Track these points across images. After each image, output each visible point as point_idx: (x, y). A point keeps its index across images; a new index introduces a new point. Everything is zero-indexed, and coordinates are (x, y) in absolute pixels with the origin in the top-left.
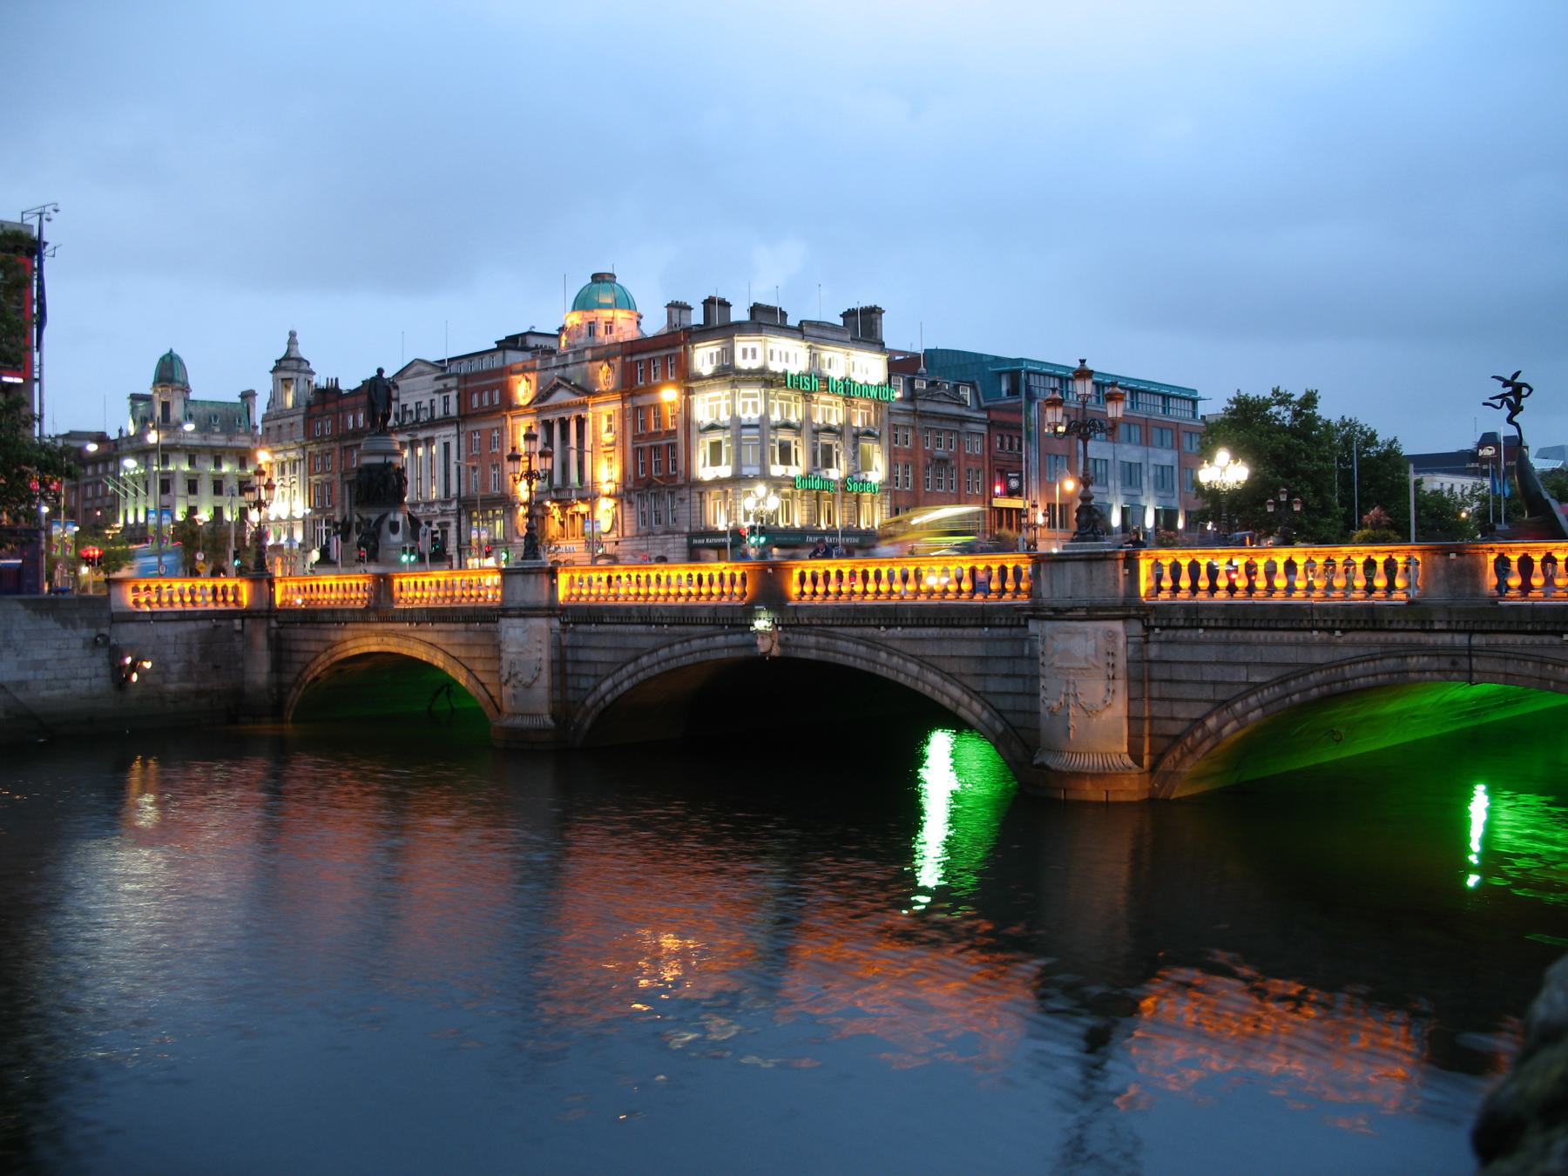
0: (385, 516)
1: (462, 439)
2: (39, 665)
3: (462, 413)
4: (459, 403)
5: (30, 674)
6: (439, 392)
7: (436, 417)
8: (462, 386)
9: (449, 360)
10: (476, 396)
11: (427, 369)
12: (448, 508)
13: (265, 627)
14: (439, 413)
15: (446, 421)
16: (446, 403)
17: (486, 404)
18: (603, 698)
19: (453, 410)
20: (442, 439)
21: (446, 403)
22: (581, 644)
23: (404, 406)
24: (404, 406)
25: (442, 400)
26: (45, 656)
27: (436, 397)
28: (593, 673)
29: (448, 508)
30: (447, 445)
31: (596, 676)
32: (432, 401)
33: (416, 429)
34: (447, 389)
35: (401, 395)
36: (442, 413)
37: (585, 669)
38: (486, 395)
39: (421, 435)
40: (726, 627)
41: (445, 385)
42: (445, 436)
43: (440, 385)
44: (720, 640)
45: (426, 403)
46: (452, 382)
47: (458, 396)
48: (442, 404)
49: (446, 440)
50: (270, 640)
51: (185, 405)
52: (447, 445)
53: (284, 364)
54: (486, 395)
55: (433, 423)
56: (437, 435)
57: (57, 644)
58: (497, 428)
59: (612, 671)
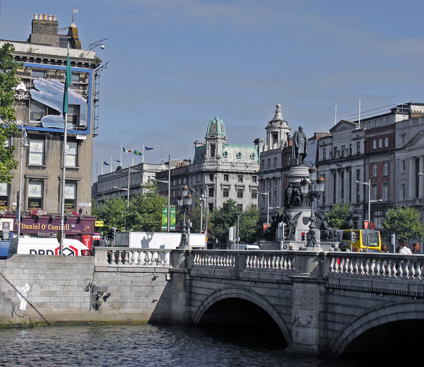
0: (300, 214)
1: (367, 168)
2: (52, 294)
3: (367, 152)
4: (365, 146)
5: (46, 299)
6: (355, 139)
7: (353, 155)
8: (367, 136)
9: (363, 121)
10: (375, 142)
11: (348, 126)
12: (358, 209)
13: (183, 279)
14: (354, 152)
15: (358, 157)
16: (358, 147)
17: (381, 146)
18: (347, 338)
19: (362, 151)
20: (355, 167)
21: (358, 147)
22: (336, 302)
23: (336, 148)
24: (336, 148)
25: (356, 144)
26: (56, 289)
27: (353, 142)
28: (342, 321)
29: (358, 209)
30: (358, 171)
31: (343, 323)
32: (351, 145)
33: (341, 161)
34: (358, 138)
35: (334, 142)
36: (356, 152)
37: (337, 318)
38: (381, 141)
39: (345, 165)
40: (415, 298)
41: (358, 136)
42: (357, 166)
43: (354, 136)
44: (412, 307)
45: (347, 147)
46: (362, 134)
47: (365, 142)
48: (356, 147)
49: (358, 168)
50: (185, 286)
51: (223, 147)
52: (358, 171)
53: (273, 124)
54: (381, 141)
55: (350, 158)
56: (353, 165)
57: (62, 283)
58: (387, 161)
59: (352, 321)
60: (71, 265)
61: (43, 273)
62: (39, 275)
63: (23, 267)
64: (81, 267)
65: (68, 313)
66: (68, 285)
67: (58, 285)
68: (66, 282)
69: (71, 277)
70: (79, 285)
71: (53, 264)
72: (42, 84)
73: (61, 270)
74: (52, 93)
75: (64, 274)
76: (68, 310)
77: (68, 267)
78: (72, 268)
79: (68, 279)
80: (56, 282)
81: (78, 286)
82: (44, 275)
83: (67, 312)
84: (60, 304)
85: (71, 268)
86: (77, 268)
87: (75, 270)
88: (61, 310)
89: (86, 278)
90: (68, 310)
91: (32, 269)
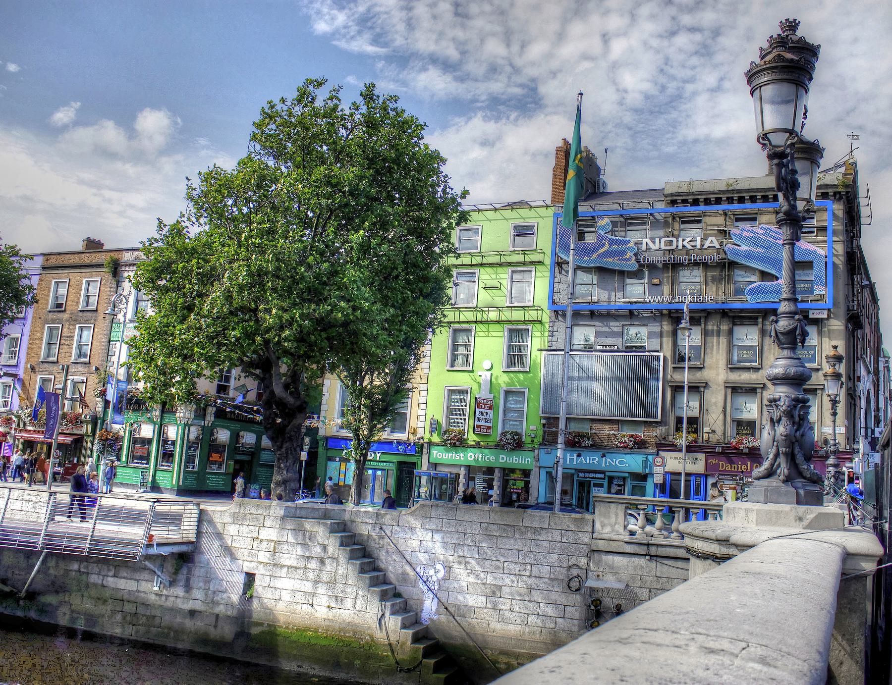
60: (535, 530)
61: (473, 544)
62: (466, 548)
63: (434, 527)
64: (558, 538)
65: (526, 637)
66: (528, 574)
67: (505, 572)
68: (522, 568)
69: (535, 559)
70: (552, 576)
71: (495, 527)
72: (745, 234)
73: (512, 541)
74: (763, 247)
75: (519, 551)
76: (527, 630)
77: (529, 535)
78: (538, 537)
79: (528, 561)
80: (501, 565)
81: (550, 579)
82: (476, 549)
83: (524, 634)
84: (507, 614)
85: (536, 538)
86: (550, 539)
87: (545, 544)
88: (513, 629)
89: (570, 564)
90: (527, 630)
91: (451, 532)
